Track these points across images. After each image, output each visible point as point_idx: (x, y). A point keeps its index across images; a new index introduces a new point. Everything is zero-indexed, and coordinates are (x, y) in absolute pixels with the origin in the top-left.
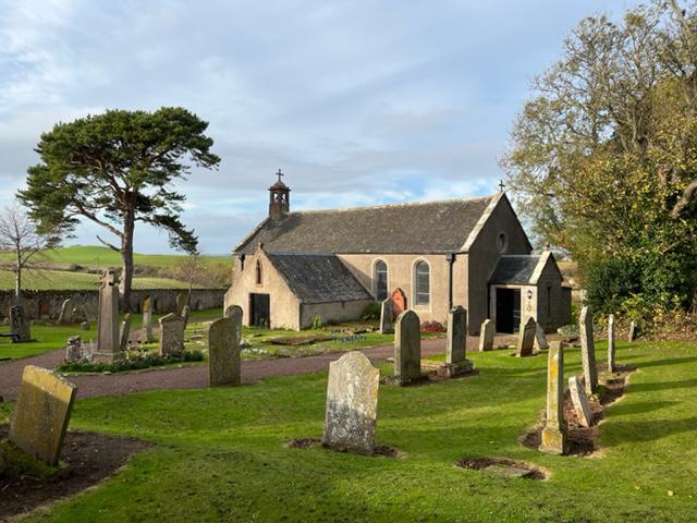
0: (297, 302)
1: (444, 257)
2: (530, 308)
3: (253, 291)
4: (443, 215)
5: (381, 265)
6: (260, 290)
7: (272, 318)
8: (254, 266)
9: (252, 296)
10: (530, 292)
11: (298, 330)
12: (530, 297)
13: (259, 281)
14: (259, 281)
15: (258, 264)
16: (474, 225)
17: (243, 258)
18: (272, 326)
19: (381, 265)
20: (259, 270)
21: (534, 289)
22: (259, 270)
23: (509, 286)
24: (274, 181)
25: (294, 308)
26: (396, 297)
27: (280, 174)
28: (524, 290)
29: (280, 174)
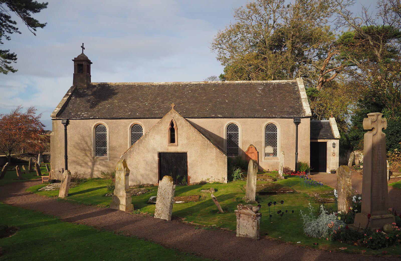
0: (224, 158)
1: (292, 120)
2: (334, 154)
3: (161, 151)
4: (263, 90)
5: (232, 128)
6: (172, 149)
7: (189, 174)
8: (168, 126)
9: (161, 155)
10: (334, 144)
11: (226, 182)
12: (334, 147)
13: (172, 140)
14: (172, 140)
15: (172, 124)
16: (299, 98)
17: (67, 124)
18: (191, 182)
19: (232, 128)
20: (172, 130)
21: (337, 142)
22: (172, 130)
23: (319, 141)
24: (77, 53)
25: (221, 163)
26: (250, 151)
27: (83, 48)
28: (330, 143)
29: (83, 48)
